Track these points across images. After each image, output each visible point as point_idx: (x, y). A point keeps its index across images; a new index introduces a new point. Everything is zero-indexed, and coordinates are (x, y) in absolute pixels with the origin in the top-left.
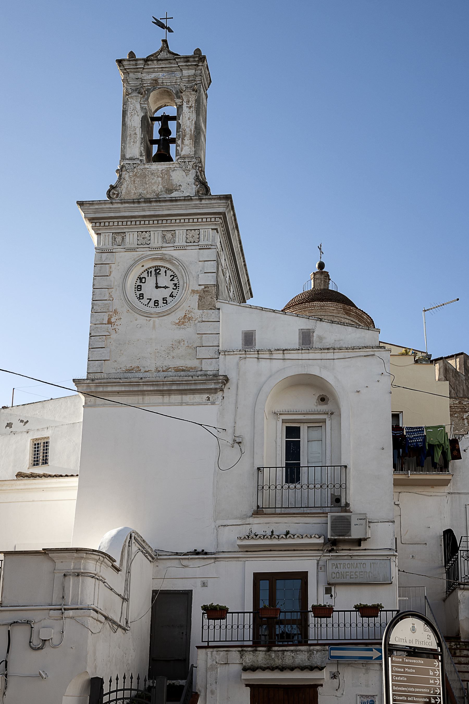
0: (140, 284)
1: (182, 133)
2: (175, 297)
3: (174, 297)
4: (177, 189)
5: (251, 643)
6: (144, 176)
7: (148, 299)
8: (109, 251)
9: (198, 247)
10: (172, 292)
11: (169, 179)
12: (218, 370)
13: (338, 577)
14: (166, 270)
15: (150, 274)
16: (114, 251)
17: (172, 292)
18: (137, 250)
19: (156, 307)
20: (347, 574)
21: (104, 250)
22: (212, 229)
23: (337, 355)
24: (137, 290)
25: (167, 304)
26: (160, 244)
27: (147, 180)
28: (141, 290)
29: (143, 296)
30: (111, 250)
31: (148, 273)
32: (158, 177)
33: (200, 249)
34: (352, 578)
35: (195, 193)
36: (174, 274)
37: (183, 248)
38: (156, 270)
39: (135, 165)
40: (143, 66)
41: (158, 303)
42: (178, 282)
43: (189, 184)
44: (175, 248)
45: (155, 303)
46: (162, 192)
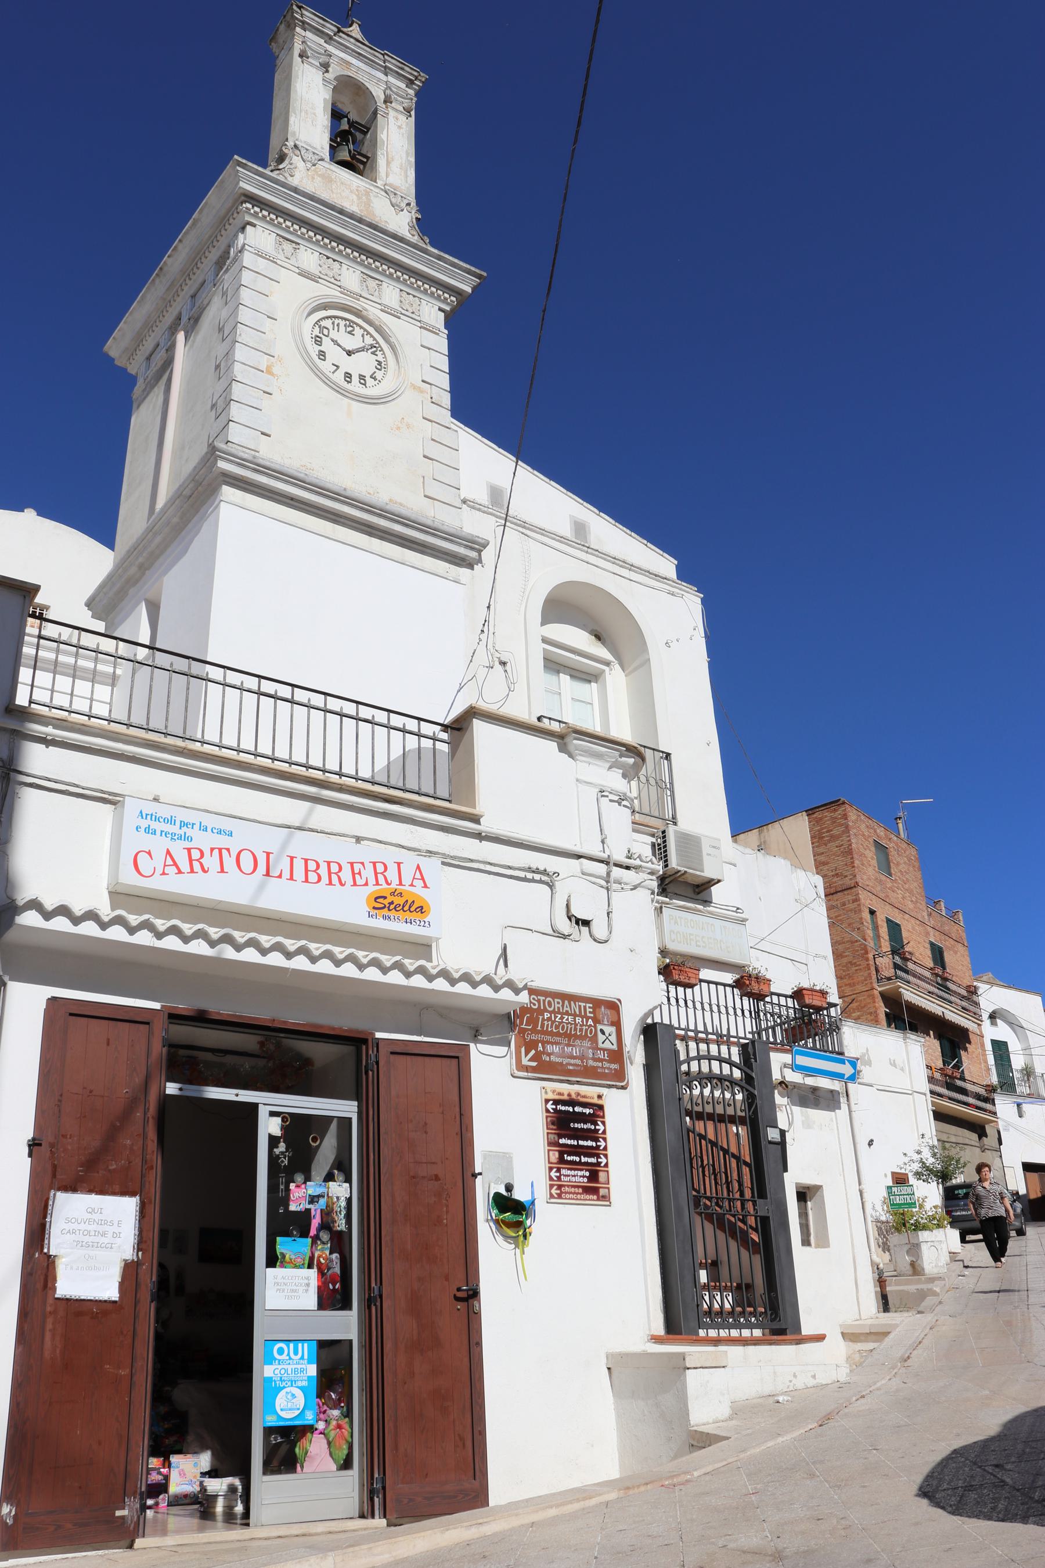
3: (377, 381)
7: (333, 364)
10: (375, 372)
13: (679, 940)
15: (336, 328)
16: (279, 262)
17: (375, 372)
18: (320, 280)
20: (692, 937)
34: (699, 946)
39: (317, 157)
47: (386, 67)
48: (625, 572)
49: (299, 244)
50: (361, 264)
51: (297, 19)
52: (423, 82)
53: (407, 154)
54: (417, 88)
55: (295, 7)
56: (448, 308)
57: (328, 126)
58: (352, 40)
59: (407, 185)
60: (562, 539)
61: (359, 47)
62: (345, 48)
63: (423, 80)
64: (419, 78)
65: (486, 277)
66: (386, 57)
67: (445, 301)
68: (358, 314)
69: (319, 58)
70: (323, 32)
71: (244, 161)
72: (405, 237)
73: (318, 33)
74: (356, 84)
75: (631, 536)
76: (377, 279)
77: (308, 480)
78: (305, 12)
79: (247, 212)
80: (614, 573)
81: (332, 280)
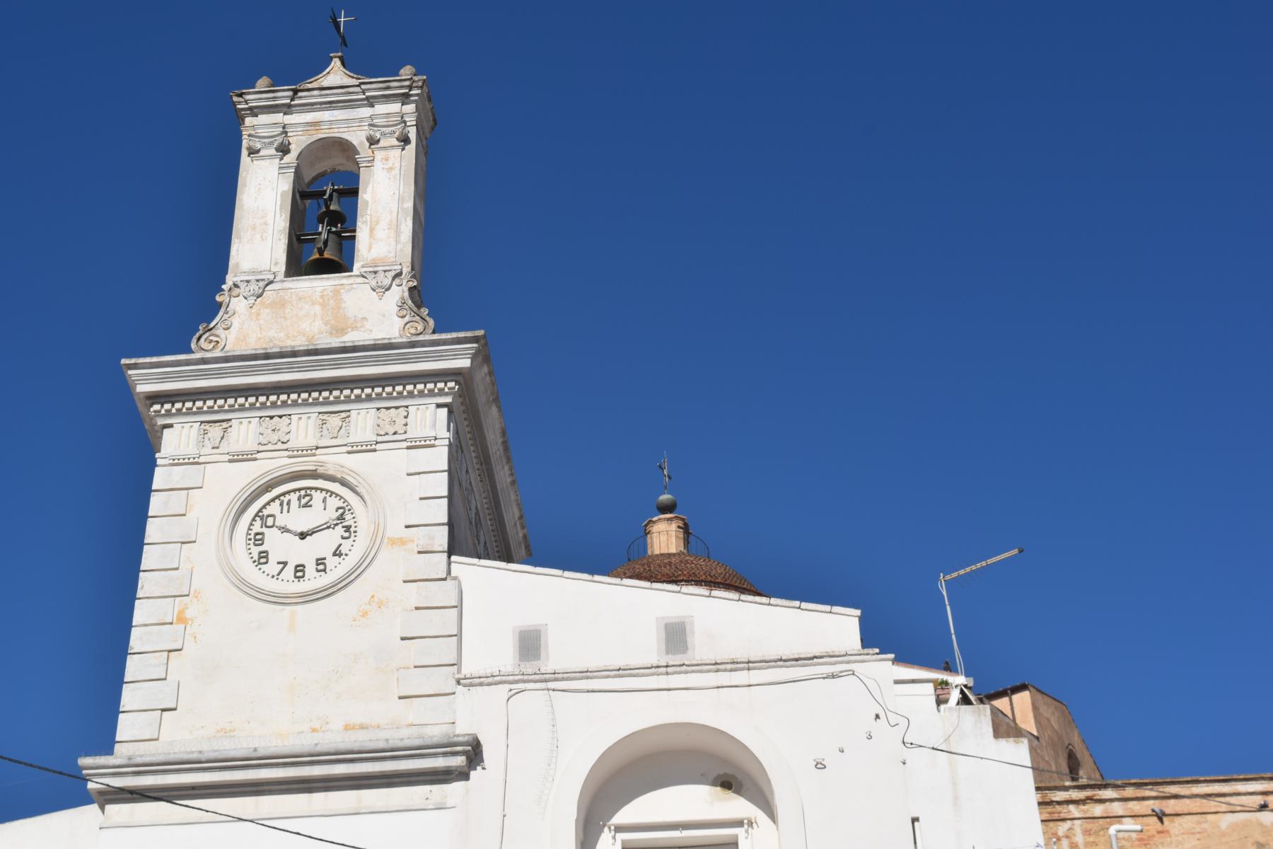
0: (260, 530)
1: (371, 219)
2: (346, 555)
3: (342, 557)
4: (356, 327)
6: (282, 304)
7: (279, 563)
8: (191, 460)
9: (405, 444)
10: (340, 545)
11: (339, 308)
12: (454, 723)
14: (325, 498)
15: (285, 507)
16: (202, 460)
17: (340, 545)
18: (259, 456)
19: (299, 581)
21: (179, 459)
22: (439, 406)
23: (756, 676)
24: (254, 543)
25: (326, 573)
26: (311, 442)
27: (287, 312)
28: (262, 544)
29: (266, 557)
30: (194, 458)
31: (281, 505)
32: (313, 304)
33: (408, 448)
35: (400, 331)
36: (342, 505)
37: (368, 448)
38: (299, 499)
40: (289, 101)
41: (303, 571)
42: (355, 522)
43: (384, 316)
44: (350, 449)
45: (296, 571)
46: (320, 333)
47: (368, 98)
48: (741, 677)
49: (230, 420)
50: (316, 403)
51: (243, 109)
52: (421, 87)
53: (401, 200)
54: (417, 98)
55: (235, 99)
56: (448, 400)
57: (284, 230)
58: (316, 93)
59: (399, 246)
60: (621, 672)
61: (327, 95)
62: (311, 107)
63: (420, 84)
64: (415, 85)
65: (484, 336)
66: (363, 87)
67: (441, 393)
68: (314, 475)
69: (271, 143)
70: (277, 106)
71: (133, 361)
72: (357, 344)
73: (272, 110)
74: (335, 142)
75: (769, 604)
76: (342, 412)
77: (203, 757)
78: (248, 97)
79: (157, 416)
80: (718, 687)
81: (280, 446)
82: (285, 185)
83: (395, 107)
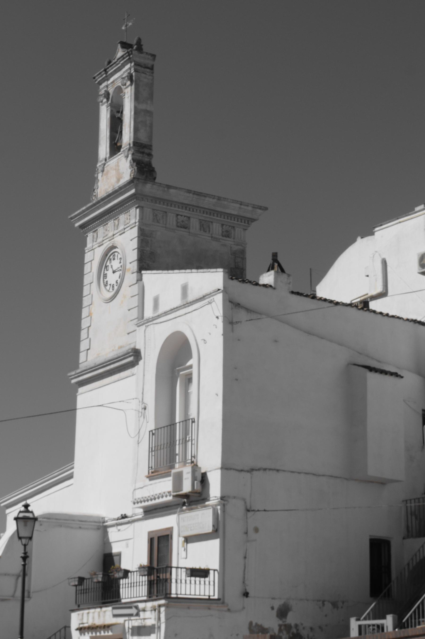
5: (145, 598)
16: (94, 247)
40: (104, 75)
82: (109, 116)
83: (128, 66)
